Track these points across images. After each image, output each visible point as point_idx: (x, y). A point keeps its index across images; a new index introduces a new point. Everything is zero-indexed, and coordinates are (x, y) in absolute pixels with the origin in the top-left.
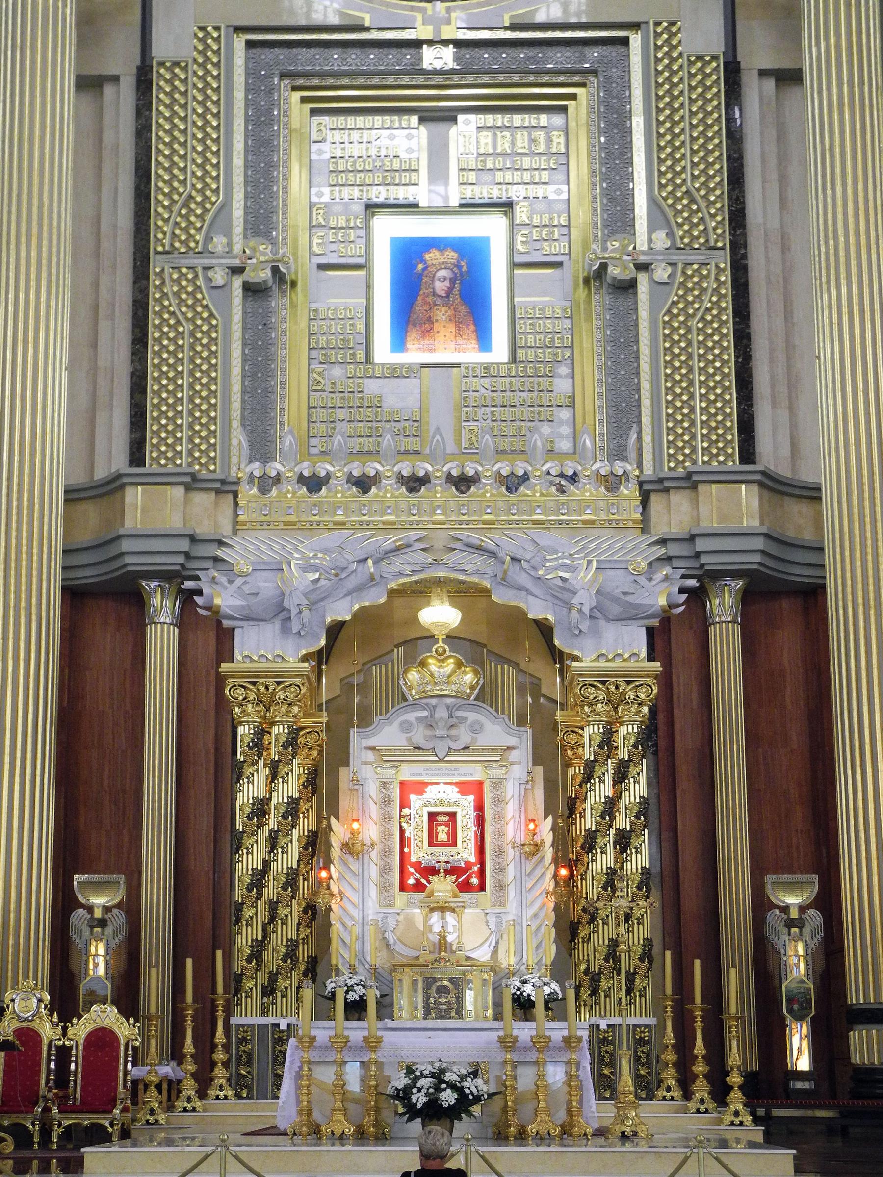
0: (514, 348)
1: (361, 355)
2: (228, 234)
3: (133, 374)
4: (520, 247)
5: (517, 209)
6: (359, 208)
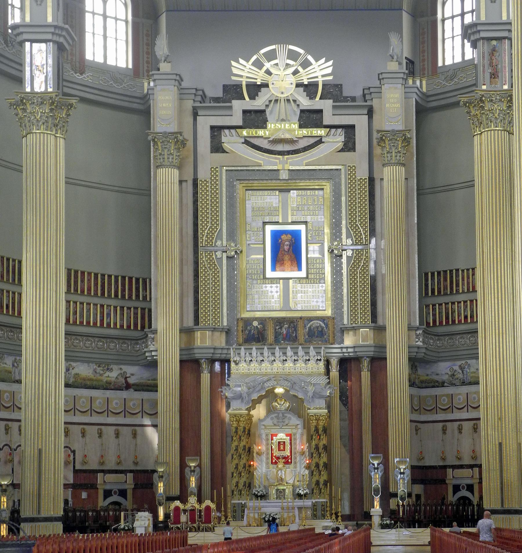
0: (308, 274)
1: (262, 277)
2: (222, 240)
3: (194, 287)
4: (309, 238)
5: (309, 225)
6: (261, 224)
